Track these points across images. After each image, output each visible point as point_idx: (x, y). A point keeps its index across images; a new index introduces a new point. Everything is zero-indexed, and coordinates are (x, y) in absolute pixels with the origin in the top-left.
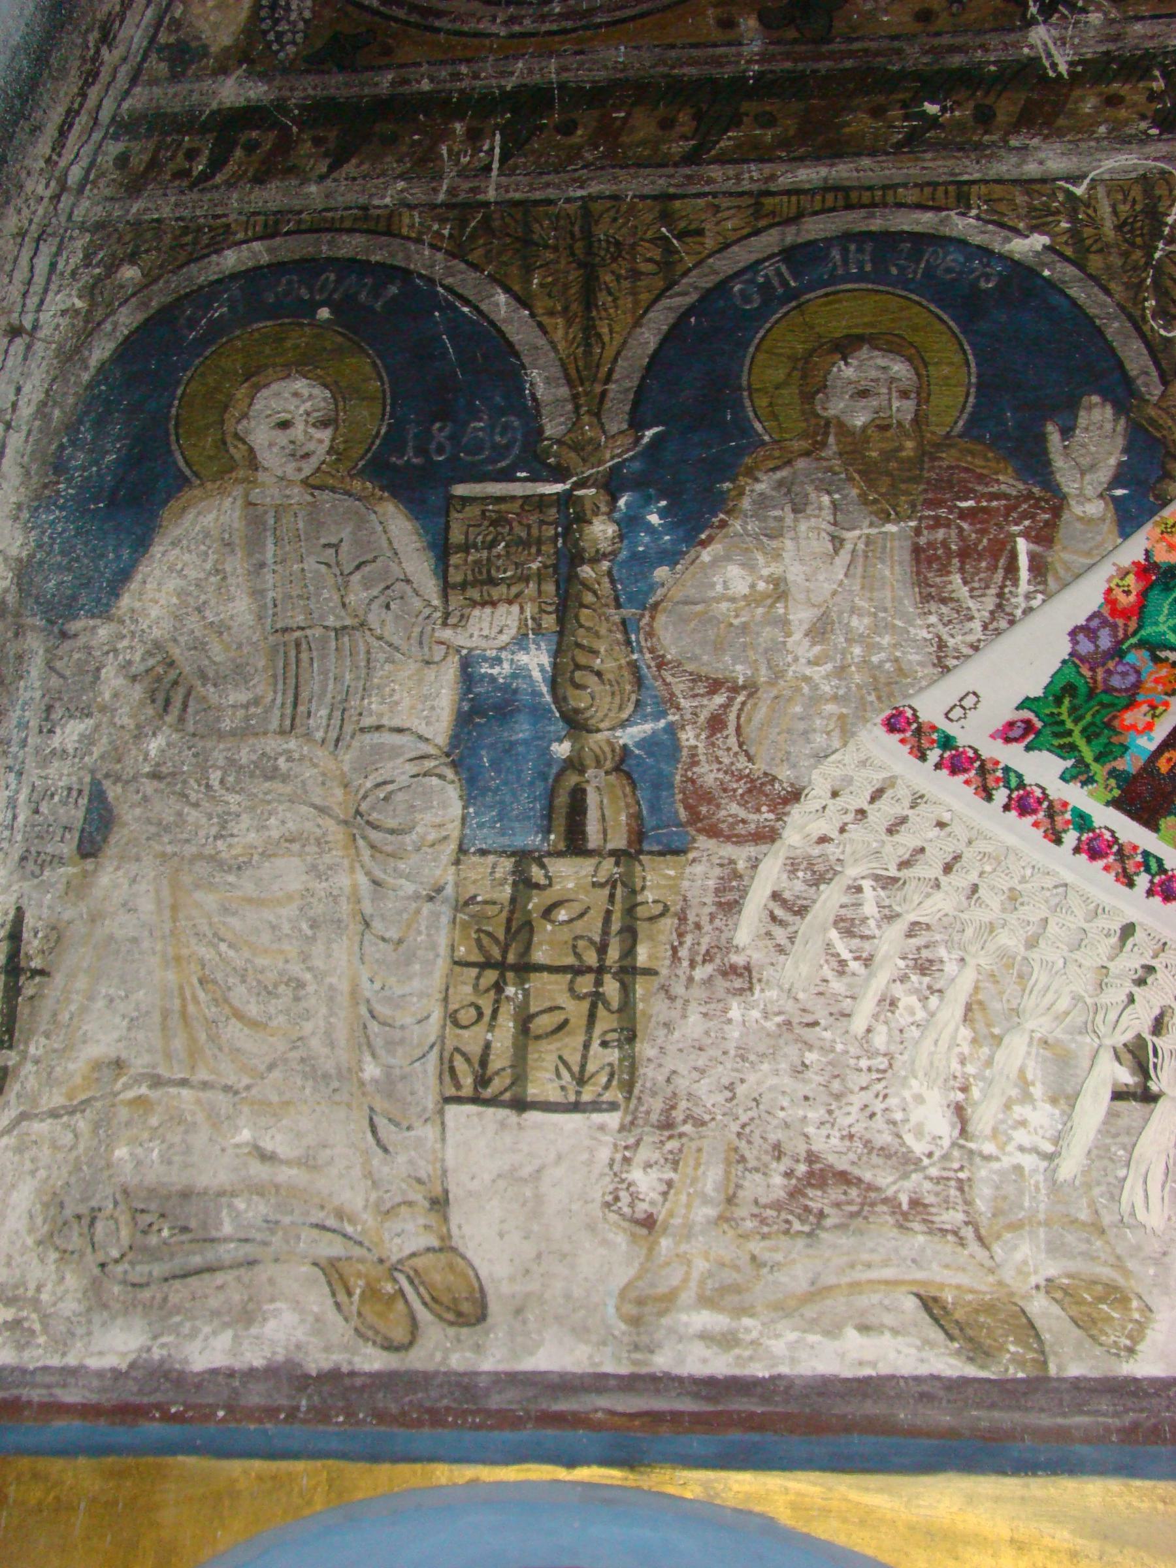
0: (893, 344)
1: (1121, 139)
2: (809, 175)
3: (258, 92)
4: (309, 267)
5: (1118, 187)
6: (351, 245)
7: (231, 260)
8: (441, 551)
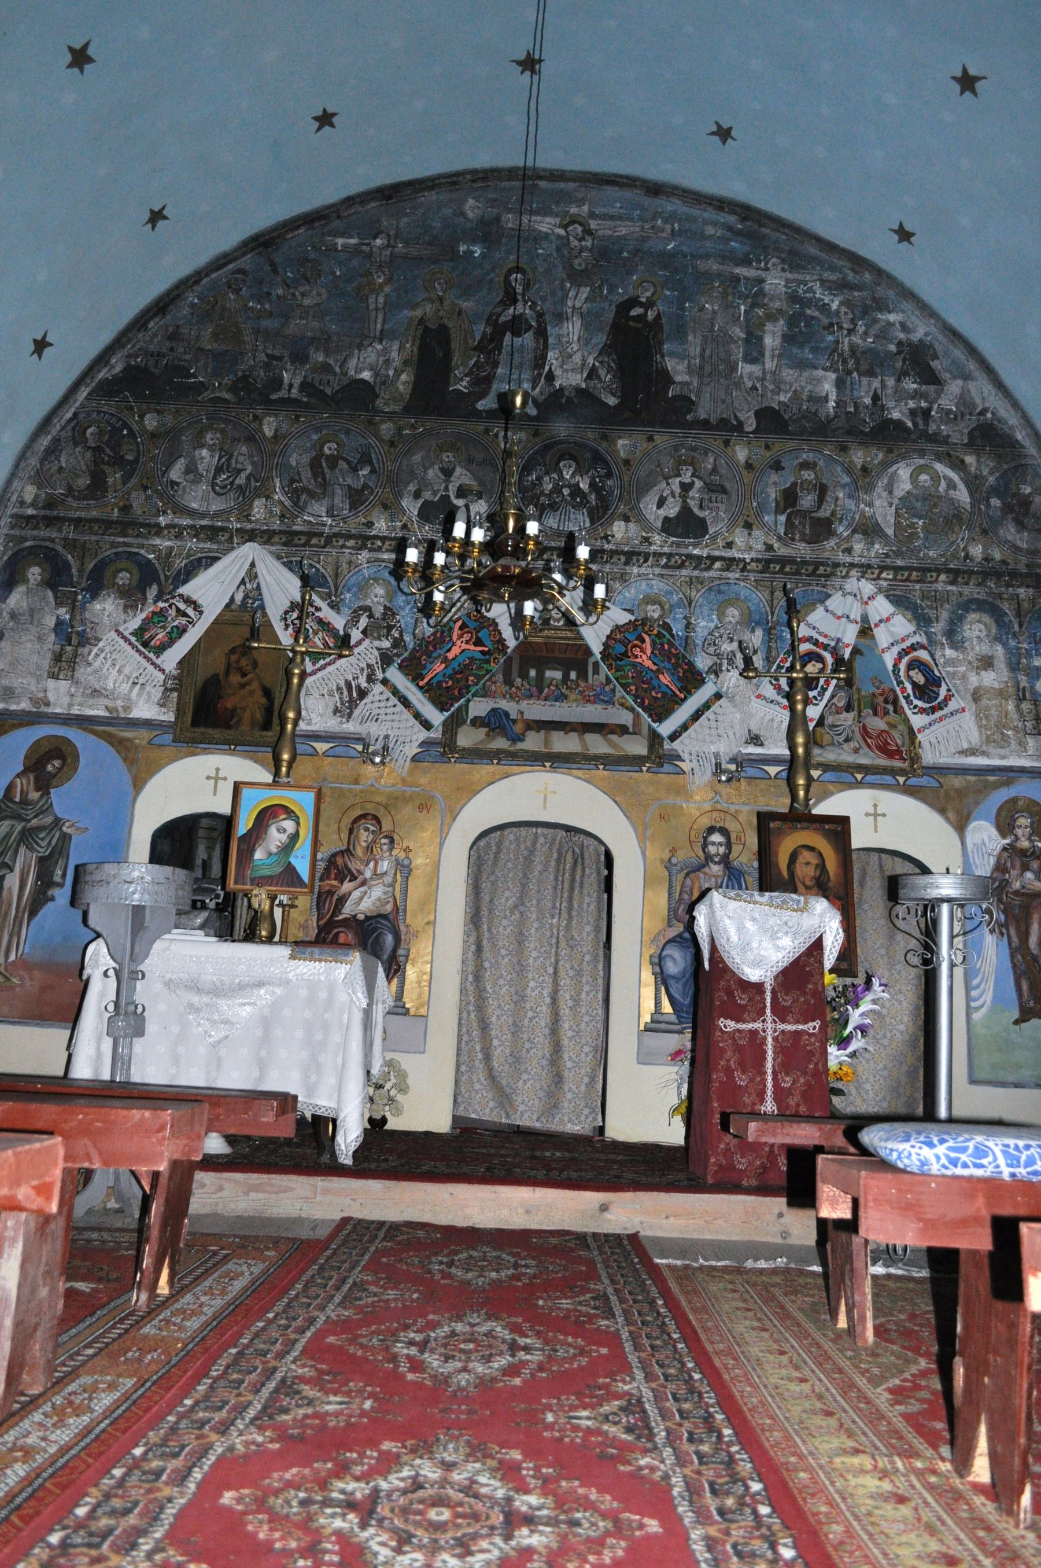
0: (127, 571)
1: (170, 539)
2: (121, 540)
3: (34, 512)
4: (40, 547)
5: (167, 547)
6: (47, 544)
7: (28, 544)
8: (56, 597)
